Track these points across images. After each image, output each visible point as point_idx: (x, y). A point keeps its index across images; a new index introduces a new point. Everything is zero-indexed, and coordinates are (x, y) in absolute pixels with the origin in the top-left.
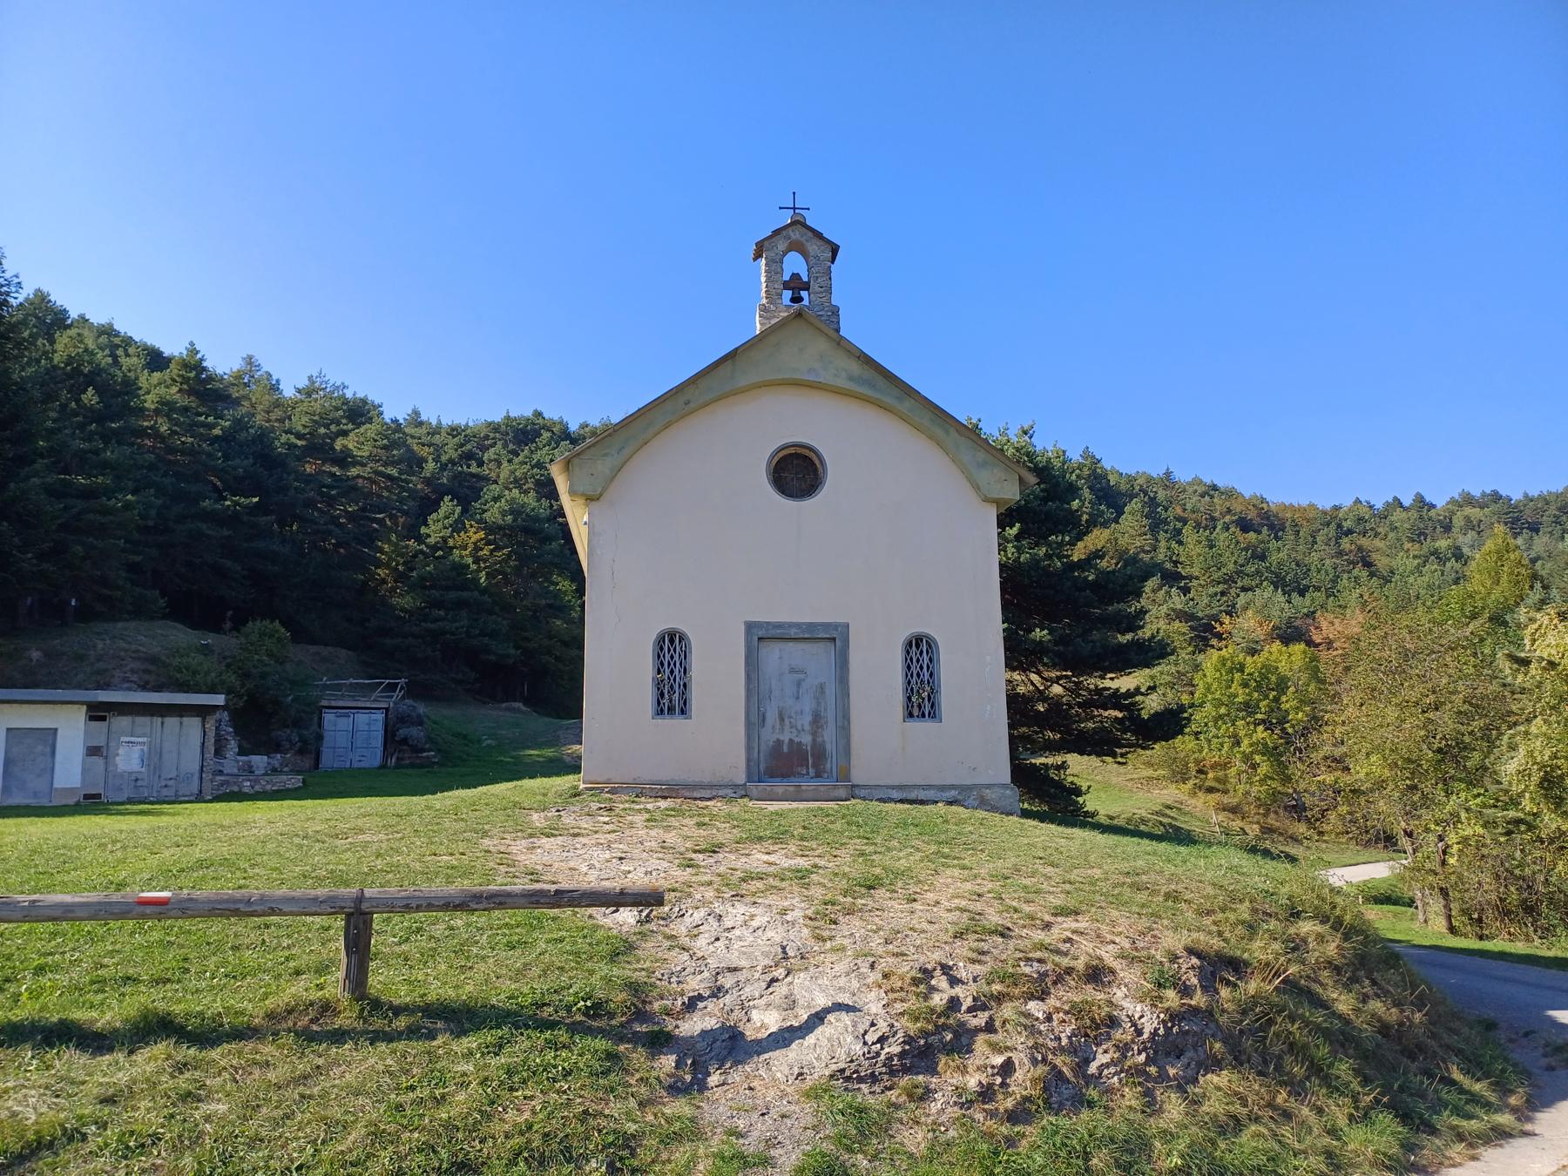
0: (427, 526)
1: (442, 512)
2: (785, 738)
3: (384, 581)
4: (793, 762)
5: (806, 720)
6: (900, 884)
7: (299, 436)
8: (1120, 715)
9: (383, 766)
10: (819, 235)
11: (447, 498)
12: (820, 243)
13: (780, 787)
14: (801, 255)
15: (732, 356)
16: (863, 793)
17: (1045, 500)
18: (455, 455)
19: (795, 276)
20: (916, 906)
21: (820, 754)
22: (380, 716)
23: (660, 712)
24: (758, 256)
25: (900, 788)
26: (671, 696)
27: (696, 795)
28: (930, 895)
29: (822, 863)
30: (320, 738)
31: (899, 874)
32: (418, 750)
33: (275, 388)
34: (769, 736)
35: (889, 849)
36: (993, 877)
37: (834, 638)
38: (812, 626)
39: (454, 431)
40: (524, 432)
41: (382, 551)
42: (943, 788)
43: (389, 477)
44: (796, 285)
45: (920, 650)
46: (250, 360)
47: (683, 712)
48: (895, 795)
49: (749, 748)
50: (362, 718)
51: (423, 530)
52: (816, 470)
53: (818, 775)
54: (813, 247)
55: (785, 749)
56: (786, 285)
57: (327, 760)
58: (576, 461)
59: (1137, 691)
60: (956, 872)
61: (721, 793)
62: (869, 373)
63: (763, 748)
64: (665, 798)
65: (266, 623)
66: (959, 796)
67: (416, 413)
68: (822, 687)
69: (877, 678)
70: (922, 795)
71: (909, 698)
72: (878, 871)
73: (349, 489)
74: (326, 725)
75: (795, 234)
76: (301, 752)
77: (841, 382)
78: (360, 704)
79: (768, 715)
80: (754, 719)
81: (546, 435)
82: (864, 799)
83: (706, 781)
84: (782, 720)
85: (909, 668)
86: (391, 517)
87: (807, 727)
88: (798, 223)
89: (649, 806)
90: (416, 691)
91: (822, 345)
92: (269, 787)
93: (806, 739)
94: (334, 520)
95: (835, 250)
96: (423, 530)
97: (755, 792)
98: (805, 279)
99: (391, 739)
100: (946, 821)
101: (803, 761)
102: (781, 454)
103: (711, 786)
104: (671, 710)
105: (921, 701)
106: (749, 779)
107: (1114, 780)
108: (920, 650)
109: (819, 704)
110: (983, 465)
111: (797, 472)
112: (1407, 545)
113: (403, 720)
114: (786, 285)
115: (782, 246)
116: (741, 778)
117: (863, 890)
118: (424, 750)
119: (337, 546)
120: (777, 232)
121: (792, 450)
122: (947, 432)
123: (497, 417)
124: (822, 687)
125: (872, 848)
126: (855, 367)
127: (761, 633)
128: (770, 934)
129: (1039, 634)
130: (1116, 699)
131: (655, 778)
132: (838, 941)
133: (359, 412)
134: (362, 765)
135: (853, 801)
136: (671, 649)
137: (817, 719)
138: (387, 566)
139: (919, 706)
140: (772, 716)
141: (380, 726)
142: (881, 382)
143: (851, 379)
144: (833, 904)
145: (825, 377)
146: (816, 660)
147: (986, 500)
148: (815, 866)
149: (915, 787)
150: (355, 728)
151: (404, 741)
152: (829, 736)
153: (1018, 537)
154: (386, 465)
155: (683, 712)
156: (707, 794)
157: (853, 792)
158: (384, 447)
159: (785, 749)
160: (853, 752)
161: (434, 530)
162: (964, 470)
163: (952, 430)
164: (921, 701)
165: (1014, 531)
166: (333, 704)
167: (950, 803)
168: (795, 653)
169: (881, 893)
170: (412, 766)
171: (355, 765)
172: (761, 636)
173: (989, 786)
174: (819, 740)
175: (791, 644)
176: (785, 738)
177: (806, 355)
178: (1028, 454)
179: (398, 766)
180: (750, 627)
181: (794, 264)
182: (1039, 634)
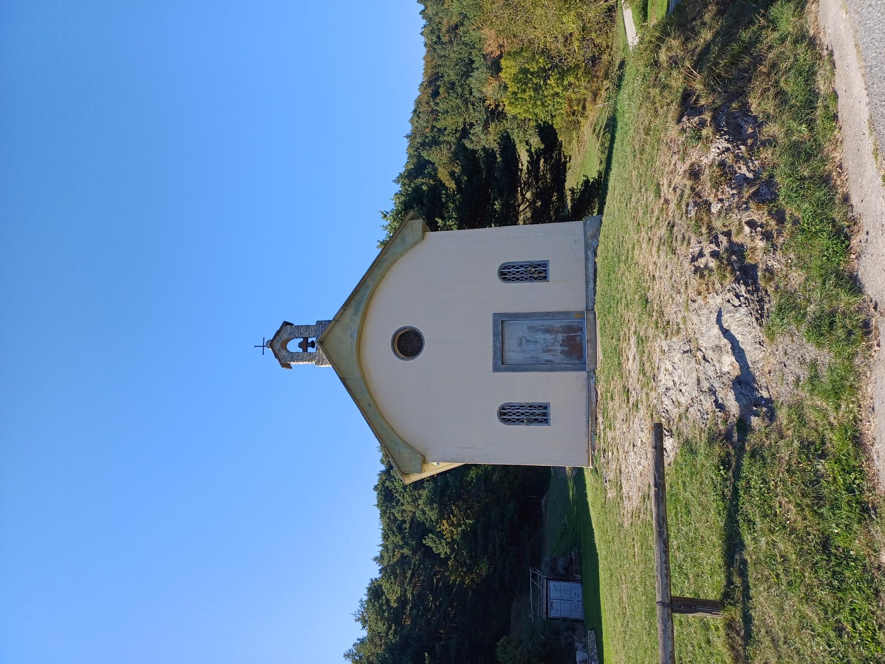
0: (440, 554)
1: (431, 545)
2: (559, 348)
3: (472, 580)
4: (573, 343)
5: (549, 337)
6: (644, 284)
7: (389, 628)
8: (542, 160)
9: (581, 582)
10: (278, 333)
11: (424, 542)
12: (282, 332)
13: (588, 352)
15: (343, 380)
16: (591, 304)
17: (422, 204)
18: (399, 537)
19: (300, 345)
20: (657, 275)
21: (569, 329)
22: (552, 584)
23: (546, 421)
24: (289, 366)
25: (587, 283)
26: (538, 414)
27: (594, 400)
28: (651, 267)
29: (633, 329)
30: (565, 619)
31: (639, 285)
32: (571, 562)
33: (362, 641)
34: (559, 358)
35: (624, 290)
36: (639, 232)
37: (501, 321)
38: (495, 334)
39: (385, 537)
40: (385, 496)
41: (455, 581)
42: (587, 259)
43: (412, 575)
44: (304, 345)
45: (508, 273)
46: (347, 656)
47: (546, 408)
48: (591, 286)
49: (566, 370)
50: (553, 594)
51: (442, 556)
52: (407, 332)
53: (581, 330)
54: (285, 336)
55: (566, 349)
56: (305, 350)
57: (577, 615)
58: (403, 469)
59: (529, 151)
60: (636, 252)
61: (593, 386)
62: (353, 303)
63: (566, 362)
64: (596, 418)
65: (498, 650)
66: (591, 249)
67: (375, 559)
68: (530, 328)
69: (524, 297)
70: (591, 271)
71: (535, 279)
72: (637, 297)
73: (420, 598)
74: (557, 615)
75: (277, 346)
76: (574, 631)
77: (358, 319)
78: (545, 595)
79: (546, 358)
80: (549, 366)
81: (387, 483)
82: (594, 303)
83: (584, 394)
84: (549, 351)
85: (518, 279)
86: (435, 574)
87: (553, 336)
88: (271, 344)
89: (602, 428)
90: (536, 563)
91: (338, 329)
92: (595, 651)
93: (560, 337)
94: (438, 608)
95: (286, 324)
96: (442, 556)
97: (592, 366)
98: (302, 340)
99: (565, 576)
100: (606, 257)
101: (573, 338)
102: (398, 352)
103: (589, 391)
104: (545, 414)
105: (537, 272)
106: (584, 369)
107: (579, 161)
108: (508, 273)
109: (539, 330)
110: (403, 240)
111: (408, 343)
112: (446, 6)
113: (553, 569)
114: (305, 350)
115: (284, 353)
116: (584, 374)
117: (649, 305)
118: (571, 558)
119: (452, 606)
120: (276, 356)
121: (396, 346)
122: (385, 260)
123: (378, 512)
124: (530, 328)
125: (624, 300)
126: (350, 311)
127: (500, 363)
128: (676, 360)
129: (497, 206)
130: (534, 162)
131: (585, 424)
132: (679, 320)
133: (375, 592)
134: (581, 595)
135: (596, 310)
136: (509, 414)
137: (548, 331)
138: (463, 578)
139: (540, 273)
140: (547, 357)
141: (557, 584)
142: (357, 298)
143: (356, 314)
144: (657, 323)
145: (355, 327)
146: (515, 332)
147: (423, 238)
148: (635, 333)
149: (586, 275)
150: (560, 598)
151: (566, 569)
152: (557, 324)
153: (443, 219)
154: (405, 577)
155: (546, 408)
156: (593, 393)
157: (590, 309)
158: (395, 578)
159: (566, 349)
160: (567, 309)
161: (442, 549)
162: (406, 251)
163: (385, 257)
164: (537, 272)
165: (440, 221)
166: (545, 611)
167: (596, 255)
168: (510, 344)
169: (650, 295)
170: (580, 565)
171: (581, 598)
172: (501, 363)
173: (585, 234)
174: (560, 329)
175: (506, 346)
176: (559, 348)
177: (342, 339)
178: (397, 215)
179: (581, 573)
180: (496, 369)
181: (294, 346)
182: (497, 206)
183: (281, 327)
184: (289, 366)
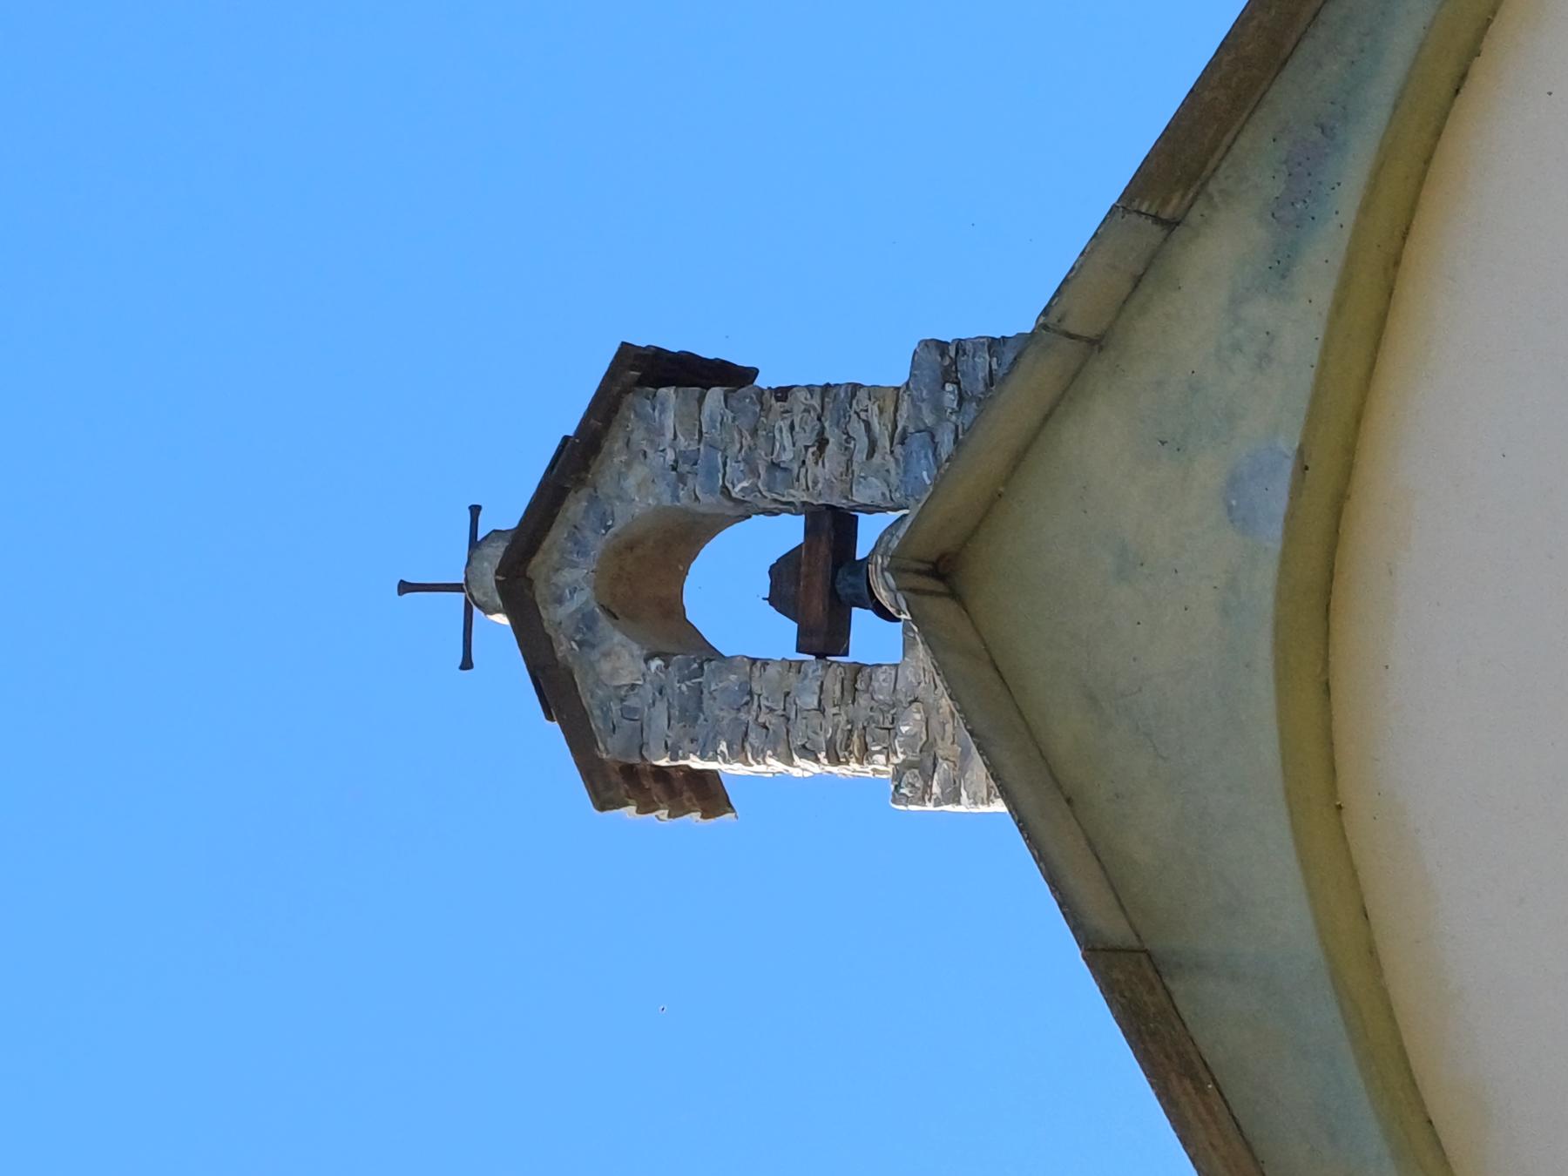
10: (575, 462)
12: (615, 450)
14: (657, 562)
24: (707, 794)
44: (819, 589)
54: (636, 488)
56: (824, 638)
75: (571, 585)
95: (645, 371)
98: (788, 532)
114: (824, 638)
115: (621, 664)
120: (556, 689)
181: (731, 593)
183: (606, 407)
184: (707, 794)
